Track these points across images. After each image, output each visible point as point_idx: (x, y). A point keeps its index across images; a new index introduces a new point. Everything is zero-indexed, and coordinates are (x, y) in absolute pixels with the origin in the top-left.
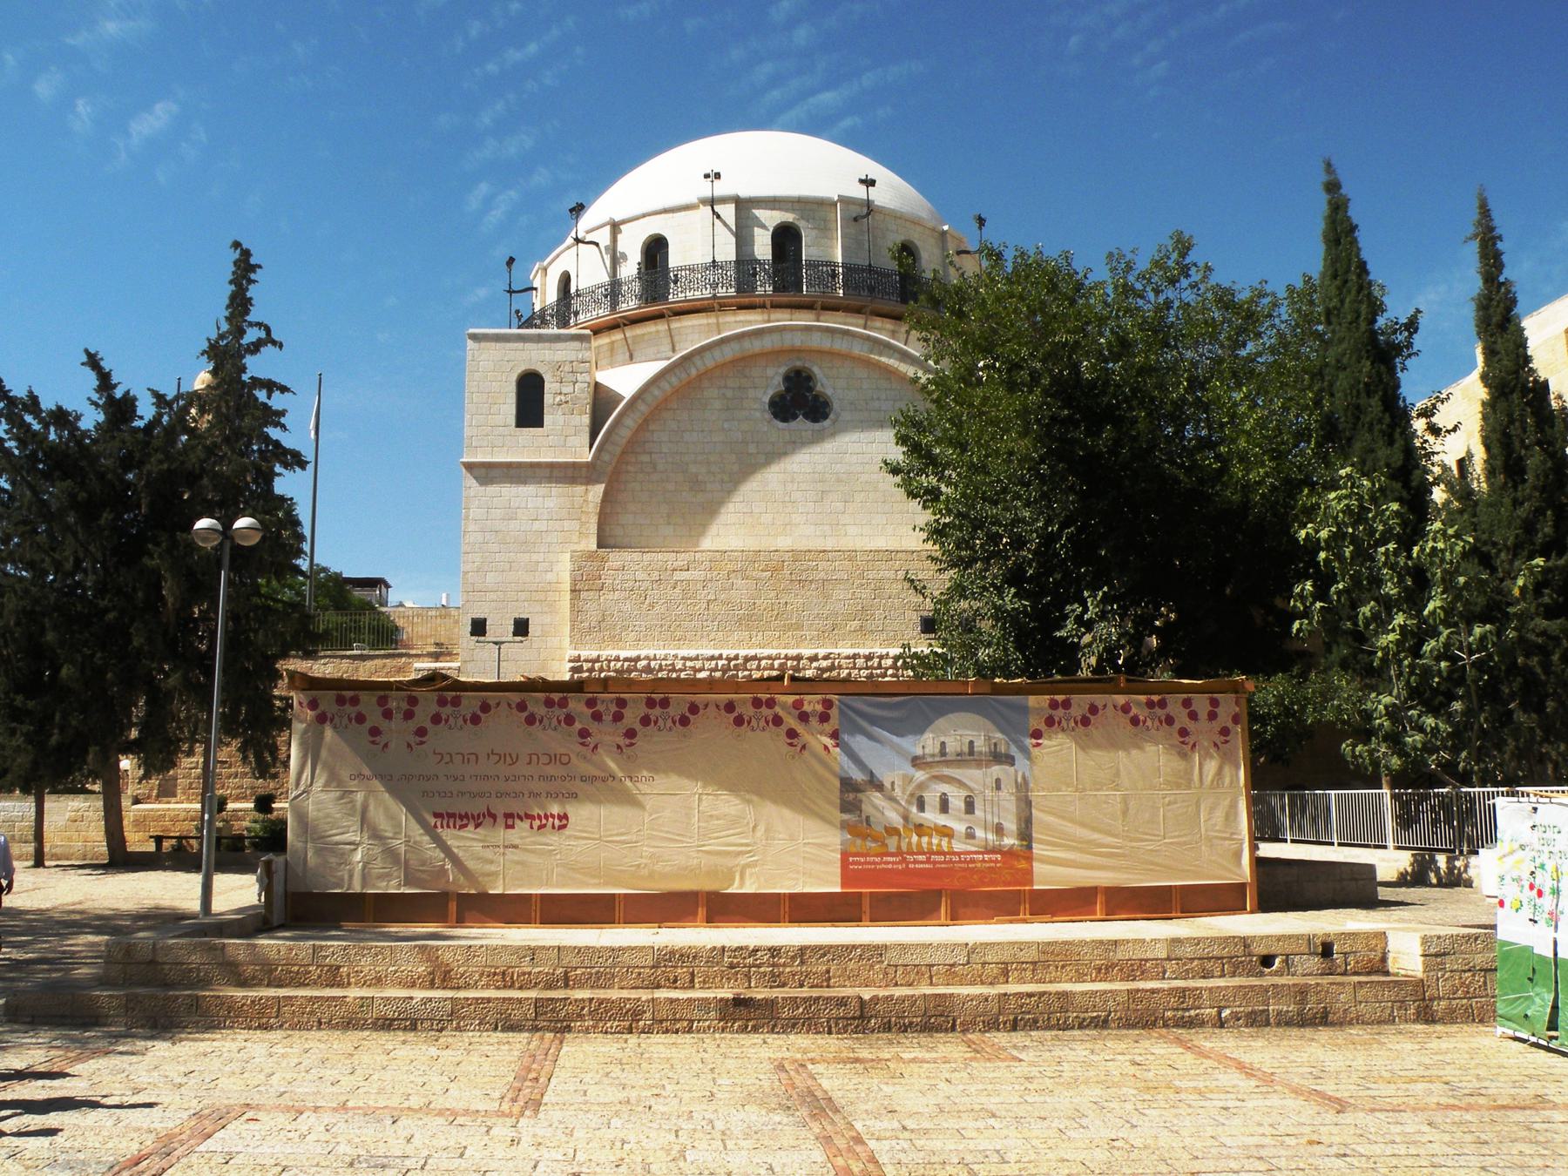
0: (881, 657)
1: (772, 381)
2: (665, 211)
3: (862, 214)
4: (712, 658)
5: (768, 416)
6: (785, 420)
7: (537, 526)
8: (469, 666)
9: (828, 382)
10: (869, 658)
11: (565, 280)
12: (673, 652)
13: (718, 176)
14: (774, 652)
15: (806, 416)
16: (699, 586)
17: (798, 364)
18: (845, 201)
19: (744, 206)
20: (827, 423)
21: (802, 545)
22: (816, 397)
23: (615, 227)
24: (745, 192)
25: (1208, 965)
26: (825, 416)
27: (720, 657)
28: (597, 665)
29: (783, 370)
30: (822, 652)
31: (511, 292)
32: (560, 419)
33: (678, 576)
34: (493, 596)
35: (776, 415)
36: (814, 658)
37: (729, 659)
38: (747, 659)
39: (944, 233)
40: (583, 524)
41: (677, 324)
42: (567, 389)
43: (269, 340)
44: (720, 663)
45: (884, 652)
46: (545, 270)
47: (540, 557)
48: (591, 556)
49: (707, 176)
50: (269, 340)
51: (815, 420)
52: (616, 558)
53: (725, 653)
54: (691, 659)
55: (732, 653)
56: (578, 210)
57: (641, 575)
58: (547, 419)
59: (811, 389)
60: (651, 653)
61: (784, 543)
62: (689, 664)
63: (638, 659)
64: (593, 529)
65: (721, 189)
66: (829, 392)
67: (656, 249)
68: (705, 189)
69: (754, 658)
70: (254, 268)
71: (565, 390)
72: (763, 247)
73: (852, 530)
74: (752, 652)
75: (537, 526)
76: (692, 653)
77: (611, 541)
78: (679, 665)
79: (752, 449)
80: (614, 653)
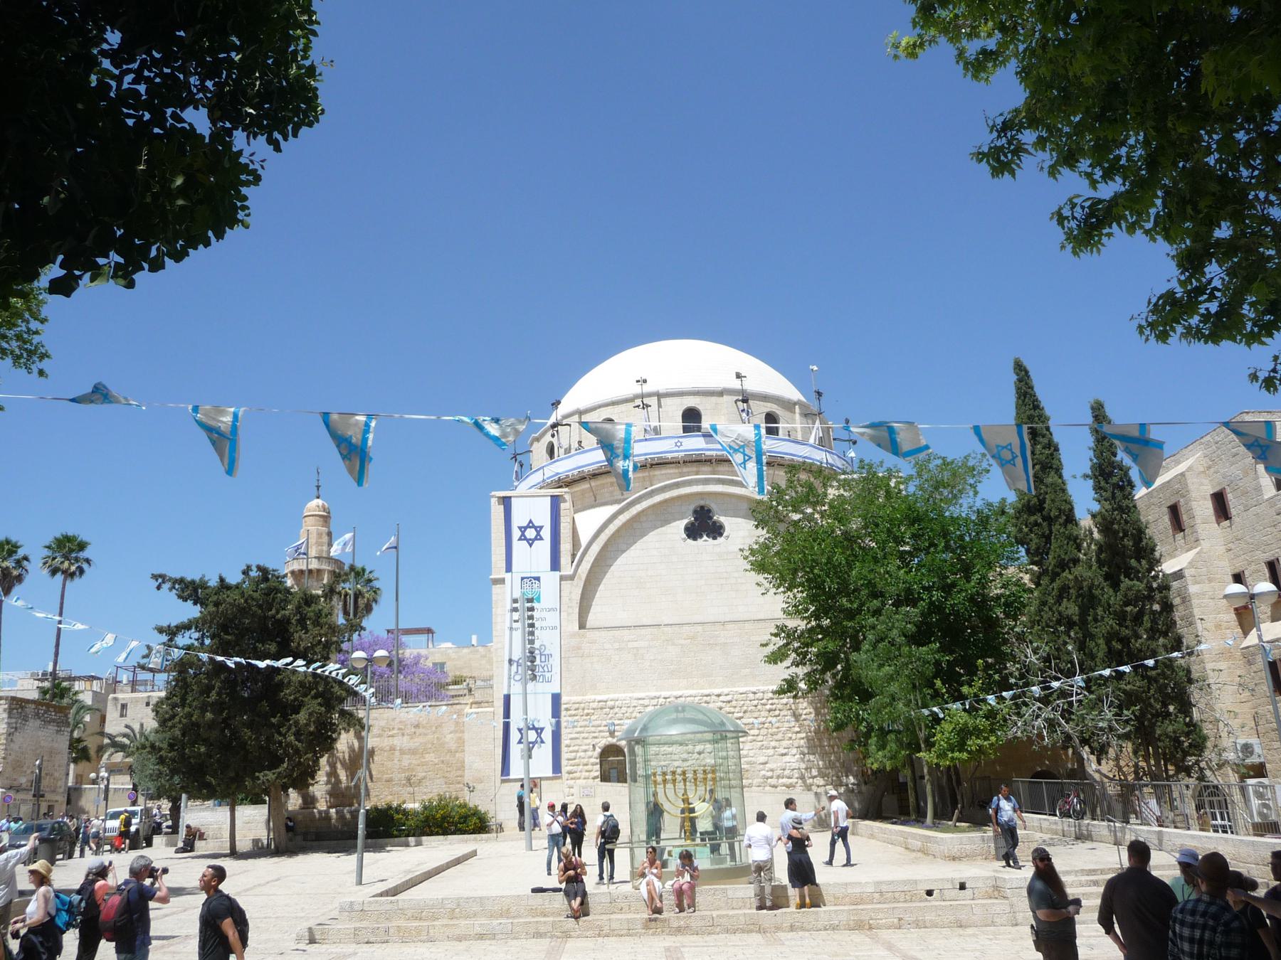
2: (613, 403)
5: (684, 536)
6: (695, 539)
13: (645, 381)
17: (702, 503)
22: (715, 523)
24: (662, 388)
25: (897, 895)
26: (721, 535)
29: (692, 507)
30: (726, 690)
33: (631, 645)
35: (689, 536)
36: (719, 696)
51: (714, 538)
56: (556, 404)
57: (607, 646)
59: (711, 518)
65: (647, 388)
68: (637, 389)
74: (679, 693)
78: (634, 703)
80: (593, 697)
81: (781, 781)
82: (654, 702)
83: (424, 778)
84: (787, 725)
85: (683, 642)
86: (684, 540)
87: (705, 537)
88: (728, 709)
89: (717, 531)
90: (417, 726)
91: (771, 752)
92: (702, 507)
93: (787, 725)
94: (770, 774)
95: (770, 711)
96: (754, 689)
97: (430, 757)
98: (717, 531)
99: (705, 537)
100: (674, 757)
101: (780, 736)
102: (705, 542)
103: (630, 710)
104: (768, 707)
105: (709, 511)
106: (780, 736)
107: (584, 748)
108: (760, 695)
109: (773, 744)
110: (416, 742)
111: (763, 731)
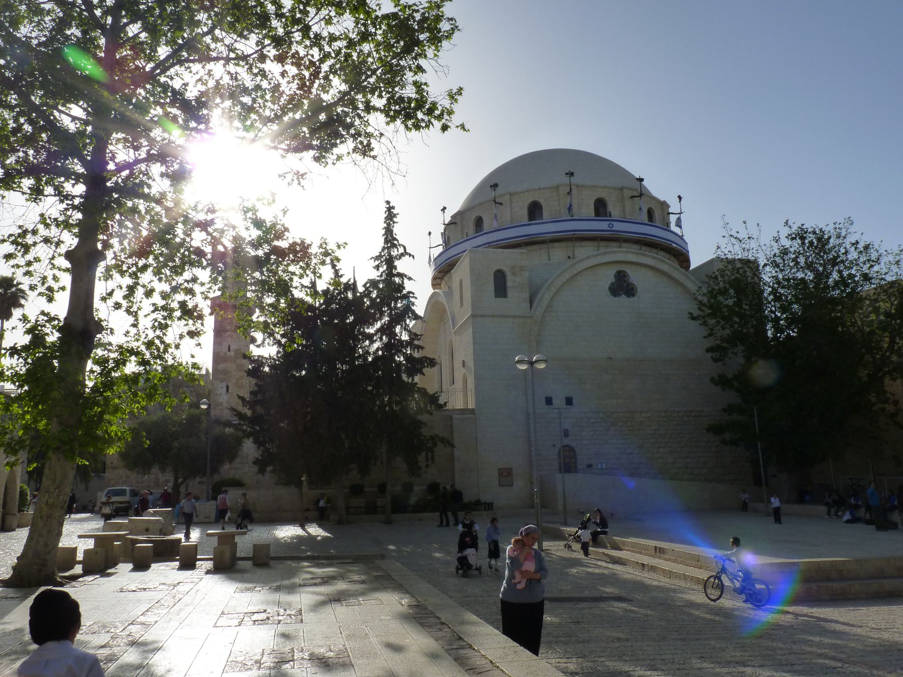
1: (608, 276)
5: (609, 293)
6: (615, 296)
9: (636, 277)
13: (572, 174)
15: (625, 294)
20: (635, 298)
22: (628, 285)
26: (633, 295)
29: (614, 272)
41: (551, 245)
43: (405, 253)
50: (405, 253)
51: (628, 296)
58: (510, 293)
59: (625, 282)
66: (635, 283)
70: (395, 216)
89: (630, 291)
98: (630, 291)
102: (623, 299)
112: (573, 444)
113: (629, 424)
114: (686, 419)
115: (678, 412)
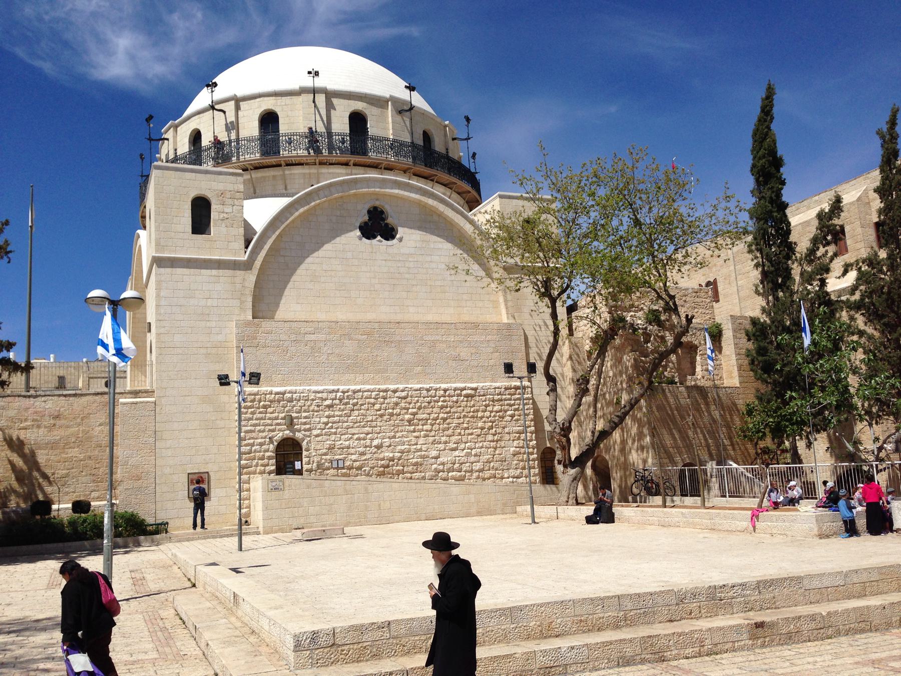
0: (436, 390)
3: (404, 109)
4: (333, 391)
6: (368, 238)
7: (209, 303)
8: (163, 400)
10: (428, 390)
11: (196, 137)
12: (308, 388)
13: (317, 74)
14: (372, 387)
16: (322, 345)
17: (377, 204)
18: (394, 100)
19: (330, 95)
20: (395, 241)
21: (384, 318)
22: (387, 225)
23: (238, 101)
24: (332, 86)
26: (393, 237)
27: (338, 391)
28: (258, 397)
30: (401, 387)
31: (150, 139)
32: (223, 229)
34: (179, 351)
36: (395, 391)
37: (344, 392)
38: (355, 392)
39: (446, 126)
40: (242, 302)
42: (228, 209)
44: (339, 394)
45: (438, 386)
46: (176, 127)
47: (213, 324)
48: (247, 324)
49: (310, 73)
51: (387, 239)
52: (266, 325)
53: (342, 388)
54: (319, 392)
55: (346, 388)
57: (283, 337)
60: (293, 388)
61: (370, 316)
62: (319, 395)
63: (284, 393)
64: (249, 305)
65: (319, 82)
67: (269, 120)
68: (308, 82)
69: (359, 391)
71: (226, 210)
72: (341, 125)
73: (411, 309)
74: (358, 387)
75: (209, 303)
76: (320, 388)
77: (260, 315)
78: (312, 396)
79: (349, 255)
80: (269, 389)
81: (450, 474)
82: (333, 395)
83: (67, 475)
84: (456, 421)
85: (360, 337)
86: (360, 239)
87: (379, 238)
88: (403, 405)
89: (389, 234)
90: (57, 417)
91: (442, 446)
92: (375, 208)
93: (456, 421)
94: (441, 467)
95: (442, 407)
96: (428, 386)
97: (74, 452)
99: (379, 238)
100: (352, 451)
101: (450, 432)
103: (309, 403)
104: (440, 404)
105: (382, 212)
106: (450, 432)
107: (259, 441)
108: (432, 392)
109: (444, 439)
110: (57, 434)
111: (436, 427)
112: (299, 435)
113: (377, 407)
114: (455, 399)
115: (445, 390)
